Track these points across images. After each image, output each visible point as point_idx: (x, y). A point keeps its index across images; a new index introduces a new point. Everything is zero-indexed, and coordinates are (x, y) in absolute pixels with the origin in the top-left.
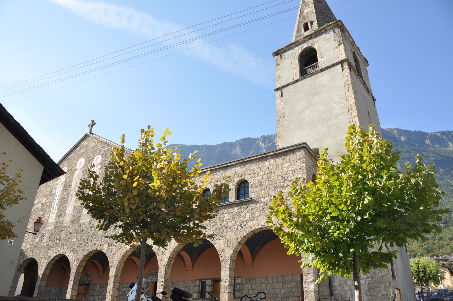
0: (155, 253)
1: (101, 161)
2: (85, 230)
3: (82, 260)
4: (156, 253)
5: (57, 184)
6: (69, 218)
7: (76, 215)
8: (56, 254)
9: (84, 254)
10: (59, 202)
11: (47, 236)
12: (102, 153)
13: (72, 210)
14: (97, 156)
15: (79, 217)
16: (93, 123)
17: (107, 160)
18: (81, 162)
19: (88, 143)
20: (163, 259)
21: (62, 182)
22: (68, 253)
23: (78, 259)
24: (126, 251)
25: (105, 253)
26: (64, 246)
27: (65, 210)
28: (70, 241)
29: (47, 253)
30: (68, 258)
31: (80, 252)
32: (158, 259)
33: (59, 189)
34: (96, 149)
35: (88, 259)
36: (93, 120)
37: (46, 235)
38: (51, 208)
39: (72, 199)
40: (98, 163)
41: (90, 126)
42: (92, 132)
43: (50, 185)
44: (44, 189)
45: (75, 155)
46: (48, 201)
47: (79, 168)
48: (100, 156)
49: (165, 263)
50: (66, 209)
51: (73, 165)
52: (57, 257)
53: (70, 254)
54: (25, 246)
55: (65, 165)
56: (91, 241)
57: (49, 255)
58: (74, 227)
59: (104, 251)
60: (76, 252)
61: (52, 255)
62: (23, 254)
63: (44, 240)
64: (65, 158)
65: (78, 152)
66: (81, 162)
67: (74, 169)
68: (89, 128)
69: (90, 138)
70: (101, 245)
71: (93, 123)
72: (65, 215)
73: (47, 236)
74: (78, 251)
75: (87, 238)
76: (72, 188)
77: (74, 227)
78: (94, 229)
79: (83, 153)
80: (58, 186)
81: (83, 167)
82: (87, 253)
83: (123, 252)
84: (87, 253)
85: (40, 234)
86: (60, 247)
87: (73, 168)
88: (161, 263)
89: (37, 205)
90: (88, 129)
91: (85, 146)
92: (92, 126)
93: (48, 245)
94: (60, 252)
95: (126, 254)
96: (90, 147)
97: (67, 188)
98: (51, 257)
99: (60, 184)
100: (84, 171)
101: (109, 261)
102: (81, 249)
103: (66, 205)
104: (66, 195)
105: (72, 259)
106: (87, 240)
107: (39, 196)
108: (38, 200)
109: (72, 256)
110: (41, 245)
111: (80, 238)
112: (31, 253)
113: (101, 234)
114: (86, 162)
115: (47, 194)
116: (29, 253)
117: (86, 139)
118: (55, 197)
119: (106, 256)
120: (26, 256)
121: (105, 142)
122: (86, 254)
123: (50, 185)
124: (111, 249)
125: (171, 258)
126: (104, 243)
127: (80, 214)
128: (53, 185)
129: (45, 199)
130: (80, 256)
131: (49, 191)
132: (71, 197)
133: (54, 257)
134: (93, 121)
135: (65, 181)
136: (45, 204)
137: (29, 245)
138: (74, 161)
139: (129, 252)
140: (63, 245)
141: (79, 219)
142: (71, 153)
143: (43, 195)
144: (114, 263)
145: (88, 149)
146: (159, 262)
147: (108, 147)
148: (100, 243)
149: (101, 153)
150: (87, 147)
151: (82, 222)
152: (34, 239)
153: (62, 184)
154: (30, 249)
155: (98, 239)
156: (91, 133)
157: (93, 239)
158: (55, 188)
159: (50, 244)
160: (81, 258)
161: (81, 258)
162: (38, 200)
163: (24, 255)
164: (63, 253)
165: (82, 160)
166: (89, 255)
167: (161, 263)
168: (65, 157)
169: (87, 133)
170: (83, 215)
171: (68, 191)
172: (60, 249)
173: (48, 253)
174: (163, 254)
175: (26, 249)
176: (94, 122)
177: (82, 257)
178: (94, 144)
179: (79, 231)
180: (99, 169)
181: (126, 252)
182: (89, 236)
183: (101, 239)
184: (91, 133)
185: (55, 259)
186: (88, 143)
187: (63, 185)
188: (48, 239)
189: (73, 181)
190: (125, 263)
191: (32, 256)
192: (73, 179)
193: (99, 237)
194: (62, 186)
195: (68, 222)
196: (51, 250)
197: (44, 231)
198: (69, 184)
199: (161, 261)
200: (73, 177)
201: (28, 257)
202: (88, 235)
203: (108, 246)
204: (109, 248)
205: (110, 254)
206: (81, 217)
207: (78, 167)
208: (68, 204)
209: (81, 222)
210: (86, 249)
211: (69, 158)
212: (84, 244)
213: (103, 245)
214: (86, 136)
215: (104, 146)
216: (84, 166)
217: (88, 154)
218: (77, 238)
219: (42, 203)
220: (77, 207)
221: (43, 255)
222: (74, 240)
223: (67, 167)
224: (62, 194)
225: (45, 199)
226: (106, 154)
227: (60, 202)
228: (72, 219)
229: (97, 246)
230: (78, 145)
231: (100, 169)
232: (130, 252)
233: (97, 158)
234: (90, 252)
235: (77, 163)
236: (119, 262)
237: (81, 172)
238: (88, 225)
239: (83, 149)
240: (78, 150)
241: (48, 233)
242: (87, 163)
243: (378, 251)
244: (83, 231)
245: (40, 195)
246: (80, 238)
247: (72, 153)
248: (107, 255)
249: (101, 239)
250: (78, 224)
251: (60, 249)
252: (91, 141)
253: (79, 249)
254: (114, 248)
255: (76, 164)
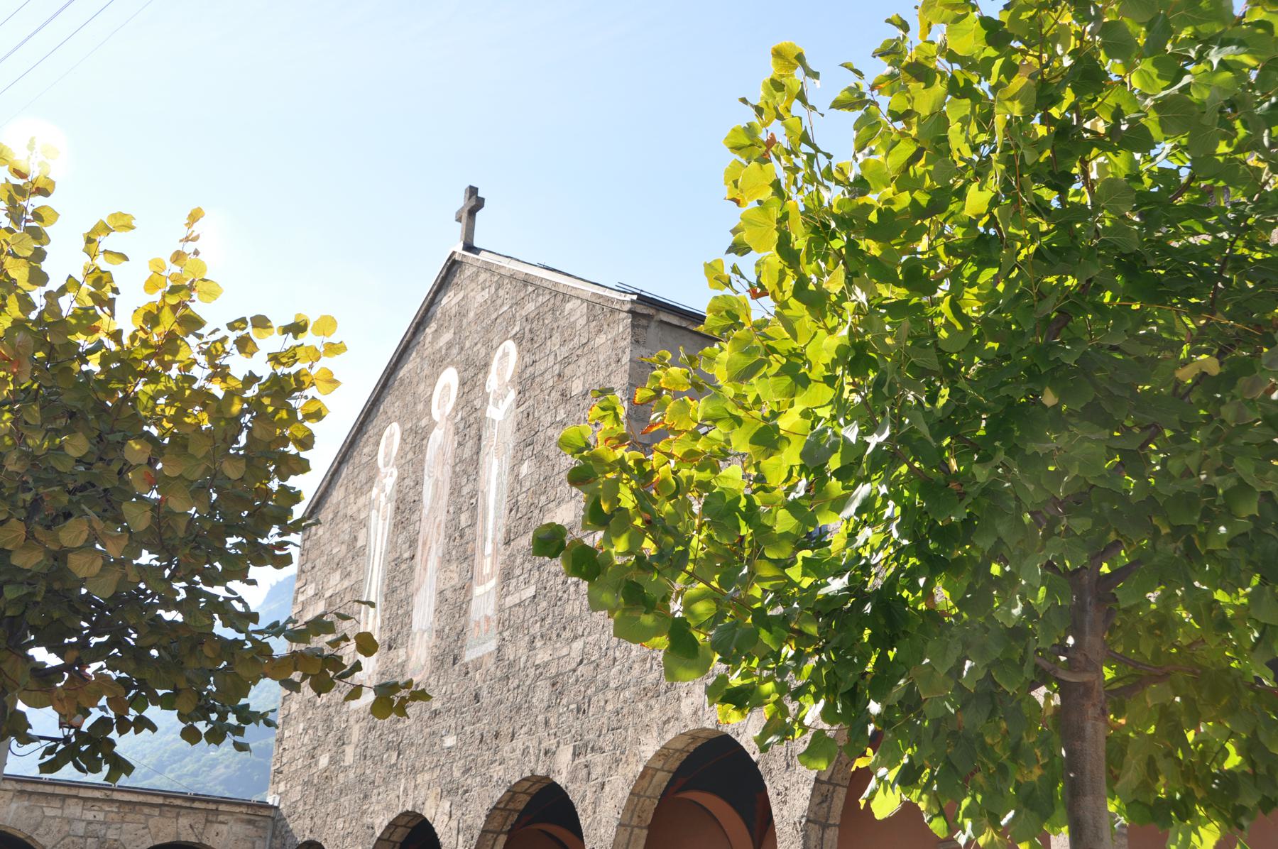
0: (756, 764)
1: (517, 367)
2: (484, 693)
3: (484, 832)
4: (760, 767)
5: (370, 504)
6: (424, 645)
7: (447, 629)
8: (391, 816)
9: (488, 804)
10: (383, 580)
11: (355, 739)
12: (517, 329)
13: (432, 609)
14: (502, 347)
15: (458, 635)
16: (474, 198)
17: (537, 358)
18: (447, 387)
19: (461, 295)
20: (791, 793)
21: (388, 490)
22: (434, 806)
23: (469, 828)
24: (641, 769)
25: (563, 786)
26: (416, 774)
27: (408, 614)
28: (437, 748)
29: (362, 814)
30: (433, 829)
31: (476, 794)
32: (769, 794)
33: (381, 522)
34: (494, 316)
35: (509, 823)
36: (471, 187)
37: (350, 734)
38: (360, 613)
39: (427, 561)
40: (508, 377)
41: (465, 215)
42: (476, 244)
43: (349, 513)
44: (328, 535)
45: (422, 359)
46: (346, 583)
47: (442, 415)
48: (510, 346)
49: (799, 813)
50: (410, 608)
51: (420, 407)
52: (397, 826)
53: (440, 810)
54: (286, 792)
55: (389, 414)
56: (509, 739)
57: (367, 820)
58: (446, 683)
59: (561, 780)
60: (459, 796)
61: (377, 822)
62: (283, 826)
63: (346, 759)
64: (390, 383)
65: (431, 343)
66: (447, 387)
67: (424, 423)
68: (459, 225)
69: (468, 272)
70: (546, 753)
71: (474, 198)
72: (408, 635)
73: (355, 739)
74: (466, 792)
75: (495, 727)
76: (425, 511)
77: (446, 683)
78: (516, 682)
79: (450, 345)
80: (374, 513)
81: (455, 409)
82: (500, 796)
83: (631, 775)
84: (499, 794)
85: (330, 735)
86: (403, 780)
87: (419, 420)
88: (785, 813)
89: (311, 608)
90: (459, 228)
91: (453, 311)
92: (472, 213)
93: (361, 779)
94: (404, 805)
95: (645, 783)
96: (471, 315)
97: (407, 514)
98: (376, 828)
99: (383, 498)
100: (461, 426)
101: (582, 822)
102: (478, 779)
103: (411, 589)
104: (407, 545)
105: (447, 829)
106: (497, 735)
107: (316, 569)
108: (313, 585)
109: (446, 818)
110: (337, 782)
111: (468, 729)
112: (308, 821)
113: (542, 700)
114: (463, 383)
115: (341, 555)
116: (301, 822)
117: (455, 280)
118: (369, 560)
119: (571, 804)
120: (293, 836)
121: (522, 277)
122: (496, 800)
123: (349, 513)
124: (586, 766)
125: (829, 782)
126: (558, 743)
127: (463, 620)
128: (359, 511)
129: (337, 576)
130: (477, 816)
131: (347, 537)
132: (426, 552)
133: (388, 827)
134: (473, 191)
135: (396, 487)
136: (338, 600)
137: (299, 788)
138: (422, 387)
139: (660, 775)
140: (414, 771)
141: (462, 647)
142: (406, 356)
143: (328, 562)
144: (603, 831)
145: (465, 321)
146: (775, 811)
147: (538, 295)
148: (544, 745)
149: (514, 332)
150: (461, 314)
151: (473, 657)
152: (313, 757)
153: (389, 500)
154: (301, 803)
155: (534, 728)
156: (469, 247)
157: (517, 727)
158: (364, 524)
159: (368, 772)
160: (479, 822)
161: (480, 823)
162: (313, 585)
163: (286, 832)
164: (414, 806)
165: (450, 378)
166: (511, 806)
167: (785, 813)
168: (387, 380)
169: (454, 253)
170: (472, 625)
171: (411, 528)
172: (405, 789)
173: (364, 812)
174: (788, 766)
175: (288, 804)
176: (480, 195)
177: (484, 818)
178: (486, 294)
179: (465, 701)
180: (514, 406)
181: (643, 775)
182: (502, 718)
183: (547, 723)
184: (469, 247)
185: (394, 838)
186: (461, 295)
187: (394, 503)
188: (358, 750)
189: (426, 477)
190: (649, 827)
191: (311, 831)
192: (423, 470)
193: (539, 719)
194: (390, 508)
195: (423, 667)
196: (374, 799)
197: (344, 718)
198: (411, 496)
199: (785, 802)
200: (423, 461)
201: (300, 840)
202: (499, 711)
203: (574, 754)
204: (576, 762)
205: (583, 788)
206: (468, 634)
207: (436, 414)
208: (415, 584)
209: (469, 656)
210: (495, 779)
211: (402, 380)
212: (487, 755)
213: (554, 753)
214: (453, 266)
215: (522, 294)
216: (457, 404)
217: (467, 344)
218: (460, 730)
219: (328, 594)
220: (448, 594)
221: (347, 825)
222: (450, 741)
223: (398, 419)
224: (393, 545)
225: (337, 576)
226: (531, 331)
227: (387, 582)
228: (435, 650)
229: (533, 758)
230: (430, 314)
231: (518, 406)
232: (662, 769)
233: (501, 358)
234: (512, 792)
235: (431, 395)
236: (620, 825)
237: (451, 432)
238: (493, 669)
239: (448, 328)
240: (429, 339)
241: (357, 726)
242: (466, 390)
243: (243, 701)
244: (477, 698)
245: (319, 563)
246: (468, 729)
247: (410, 355)
248: (575, 798)
249: (547, 723)
250: (457, 667)
251: (402, 789)
252: (473, 285)
253: (469, 781)
254: (598, 758)
255: (430, 401)
